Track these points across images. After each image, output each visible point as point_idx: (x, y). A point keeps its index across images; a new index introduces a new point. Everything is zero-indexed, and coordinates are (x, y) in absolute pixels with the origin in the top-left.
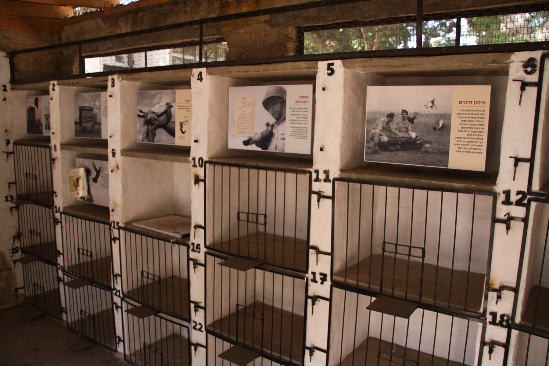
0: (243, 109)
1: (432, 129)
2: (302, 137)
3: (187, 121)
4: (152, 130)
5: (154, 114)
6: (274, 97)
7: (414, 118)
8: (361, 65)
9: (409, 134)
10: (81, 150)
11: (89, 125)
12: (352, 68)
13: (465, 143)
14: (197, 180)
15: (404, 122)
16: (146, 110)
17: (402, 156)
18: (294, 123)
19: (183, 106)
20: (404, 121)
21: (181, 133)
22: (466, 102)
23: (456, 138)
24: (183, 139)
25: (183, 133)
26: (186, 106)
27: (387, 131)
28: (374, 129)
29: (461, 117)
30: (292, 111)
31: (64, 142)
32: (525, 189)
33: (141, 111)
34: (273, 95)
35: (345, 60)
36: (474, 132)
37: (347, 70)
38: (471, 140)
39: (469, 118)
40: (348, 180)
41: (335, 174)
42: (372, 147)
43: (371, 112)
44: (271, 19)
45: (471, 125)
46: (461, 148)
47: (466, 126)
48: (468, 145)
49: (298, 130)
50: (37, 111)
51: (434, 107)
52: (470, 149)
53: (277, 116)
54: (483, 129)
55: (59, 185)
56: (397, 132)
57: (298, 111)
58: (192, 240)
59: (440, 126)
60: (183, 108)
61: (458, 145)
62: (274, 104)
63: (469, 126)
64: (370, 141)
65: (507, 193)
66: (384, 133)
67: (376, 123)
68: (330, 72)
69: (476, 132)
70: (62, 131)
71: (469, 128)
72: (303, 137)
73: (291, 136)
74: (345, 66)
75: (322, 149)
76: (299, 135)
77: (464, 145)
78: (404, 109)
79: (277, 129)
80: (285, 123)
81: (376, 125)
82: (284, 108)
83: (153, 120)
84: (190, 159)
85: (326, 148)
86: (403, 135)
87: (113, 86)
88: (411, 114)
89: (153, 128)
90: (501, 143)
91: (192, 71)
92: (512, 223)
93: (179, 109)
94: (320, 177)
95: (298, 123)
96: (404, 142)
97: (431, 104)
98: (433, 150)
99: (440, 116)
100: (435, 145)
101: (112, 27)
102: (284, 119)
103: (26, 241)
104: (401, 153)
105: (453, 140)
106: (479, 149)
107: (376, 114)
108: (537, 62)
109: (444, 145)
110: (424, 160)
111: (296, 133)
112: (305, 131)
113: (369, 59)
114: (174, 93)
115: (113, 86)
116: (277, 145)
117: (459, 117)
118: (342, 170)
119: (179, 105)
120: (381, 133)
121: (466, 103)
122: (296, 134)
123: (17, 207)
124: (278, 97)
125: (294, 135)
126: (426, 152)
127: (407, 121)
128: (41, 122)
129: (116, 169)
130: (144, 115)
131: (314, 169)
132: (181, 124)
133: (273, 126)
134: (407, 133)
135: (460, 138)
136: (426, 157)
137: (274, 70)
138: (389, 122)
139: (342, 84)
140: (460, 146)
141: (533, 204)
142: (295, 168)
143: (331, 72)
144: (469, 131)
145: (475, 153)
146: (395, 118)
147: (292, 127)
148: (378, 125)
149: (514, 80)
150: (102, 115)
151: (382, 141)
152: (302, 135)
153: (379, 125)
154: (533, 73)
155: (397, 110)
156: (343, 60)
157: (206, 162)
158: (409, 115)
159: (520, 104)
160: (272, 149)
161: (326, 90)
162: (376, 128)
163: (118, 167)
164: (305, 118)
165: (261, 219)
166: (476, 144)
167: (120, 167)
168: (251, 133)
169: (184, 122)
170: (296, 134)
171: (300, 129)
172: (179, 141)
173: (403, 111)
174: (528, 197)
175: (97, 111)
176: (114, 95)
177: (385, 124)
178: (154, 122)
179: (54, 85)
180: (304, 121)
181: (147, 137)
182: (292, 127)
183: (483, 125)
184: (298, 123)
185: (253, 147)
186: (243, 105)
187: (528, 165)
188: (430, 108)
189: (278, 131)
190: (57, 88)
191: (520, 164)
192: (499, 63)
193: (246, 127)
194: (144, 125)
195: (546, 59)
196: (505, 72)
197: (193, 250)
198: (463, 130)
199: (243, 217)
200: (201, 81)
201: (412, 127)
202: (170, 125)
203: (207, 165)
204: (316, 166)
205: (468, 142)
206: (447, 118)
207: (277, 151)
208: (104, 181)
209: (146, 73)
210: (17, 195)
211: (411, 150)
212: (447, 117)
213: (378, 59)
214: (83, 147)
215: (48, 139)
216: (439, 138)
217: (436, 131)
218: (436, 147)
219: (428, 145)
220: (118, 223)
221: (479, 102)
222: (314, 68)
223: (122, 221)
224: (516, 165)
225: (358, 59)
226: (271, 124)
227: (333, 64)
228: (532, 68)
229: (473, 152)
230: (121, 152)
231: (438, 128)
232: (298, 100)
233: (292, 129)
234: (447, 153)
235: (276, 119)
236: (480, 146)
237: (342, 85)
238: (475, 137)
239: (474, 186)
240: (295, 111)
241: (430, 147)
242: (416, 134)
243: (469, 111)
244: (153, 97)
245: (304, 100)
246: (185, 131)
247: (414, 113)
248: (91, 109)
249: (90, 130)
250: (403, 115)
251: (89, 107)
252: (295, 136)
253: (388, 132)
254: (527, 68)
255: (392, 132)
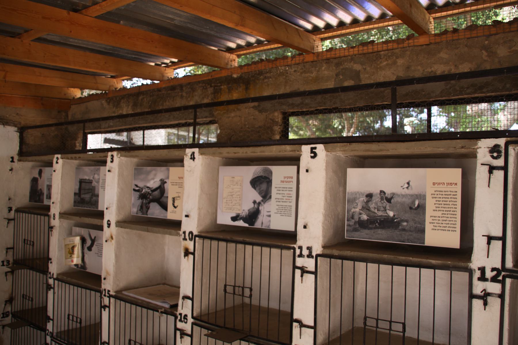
0: (232, 187)
1: (408, 209)
2: (286, 215)
3: (179, 197)
5: (148, 189)
6: (261, 177)
7: (392, 198)
8: (342, 149)
9: (387, 213)
10: (78, 219)
11: (87, 197)
12: (333, 152)
13: (440, 222)
14: (187, 253)
15: (383, 202)
16: (141, 185)
17: (381, 234)
18: (279, 202)
19: (176, 183)
20: (382, 200)
21: (173, 207)
22: (439, 184)
23: (431, 216)
24: (174, 213)
25: (175, 207)
26: (179, 183)
27: (366, 210)
28: (354, 208)
29: (435, 198)
30: (277, 190)
31: (62, 211)
32: (499, 266)
33: (137, 186)
34: (260, 175)
35: (327, 145)
36: (448, 211)
37: (329, 153)
38: (445, 219)
39: (443, 198)
40: (330, 257)
41: (318, 250)
42: (353, 225)
43: (351, 193)
44: (259, 106)
45: (445, 204)
46: (436, 226)
47: (440, 206)
48: (443, 224)
49: (283, 208)
50: (40, 182)
51: (409, 188)
52: (445, 227)
53: (263, 194)
54: (456, 208)
55: (55, 252)
56: (376, 211)
57: (283, 190)
58: (180, 310)
59: (416, 206)
60: (176, 184)
61: (433, 223)
62: (261, 183)
63: (443, 206)
64: (351, 219)
65: (482, 270)
66: (363, 211)
67: (356, 203)
68: (313, 155)
69: (450, 211)
70: (62, 202)
71: (443, 207)
72: (288, 215)
73: (276, 213)
74: (327, 150)
75: (305, 227)
76: (284, 213)
77: (439, 223)
78: (382, 190)
79: (263, 207)
80: (271, 201)
81: (356, 204)
82: (270, 188)
83: (148, 195)
84: (181, 232)
85: (310, 226)
86: (382, 214)
87: (112, 162)
88: (388, 195)
89: (147, 202)
90: (474, 222)
91: (185, 151)
92: (489, 299)
93: (172, 185)
94: (303, 253)
95: (283, 202)
96: (383, 220)
97: (406, 185)
98: (410, 228)
99: (415, 196)
100: (412, 223)
101: (115, 108)
102: (270, 197)
103: (17, 305)
104: (380, 231)
105: (428, 219)
106: (453, 227)
107: (356, 195)
108: (502, 148)
109: (420, 224)
110: (402, 237)
111: (281, 210)
112: (289, 209)
113: (349, 144)
114: (168, 170)
115: (112, 162)
116: (263, 222)
117: (433, 198)
118: (324, 247)
119: (172, 181)
120: (361, 211)
121: (439, 184)
122: (281, 211)
123: (12, 272)
124: (265, 176)
125: (280, 212)
126: (404, 230)
127: (385, 201)
128: (43, 192)
129: (110, 239)
130: (139, 189)
131: (298, 246)
132: (174, 200)
133: (259, 204)
134: (385, 212)
135: (435, 217)
136: (403, 235)
137: (261, 152)
138: (368, 202)
139: (325, 166)
140: (435, 225)
141: (508, 281)
142: (280, 244)
143: (314, 155)
144: (443, 211)
145: (449, 231)
146: (373, 198)
147: (277, 205)
148: (358, 204)
149: (482, 164)
150: (100, 188)
151: (362, 220)
152: (287, 213)
153: (359, 204)
154: (499, 158)
155: (375, 190)
156: (325, 145)
157: (196, 236)
158: (386, 195)
159: (489, 186)
160: (258, 225)
161: (309, 171)
162: (356, 207)
163: (112, 238)
164: (289, 197)
165: (247, 292)
166: (450, 222)
167: (114, 237)
168: (239, 210)
169: (176, 197)
170: (281, 211)
171: (285, 207)
172: (171, 215)
173: (381, 192)
174: (503, 273)
175: (96, 184)
176: (113, 170)
177: (364, 203)
179: (57, 158)
180: (288, 199)
181: (141, 210)
182: (277, 205)
183: (456, 205)
184: (283, 202)
185: (241, 223)
186: (232, 183)
187: (500, 242)
188: (406, 188)
189: (264, 209)
190: (60, 161)
191: (493, 242)
192: (468, 148)
193: (234, 204)
194: (139, 199)
195: (509, 146)
196: (474, 156)
197: (180, 320)
198: (438, 209)
199: (230, 289)
200: (194, 160)
201: (389, 207)
202: (163, 199)
203: (197, 238)
204: (299, 243)
205: (443, 220)
206: (422, 198)
207: (263, 227)
208: (99, 250)
209: (143, 151)
210: (14, 260)
211: (389, 228)
212: (422, 197)
213: (357, 144)
214: (80, 217)
215: (48, 208)
216: (416, 217)
217: (412, 210)
218: (413, 225)
219: (405, 224)
220: (109, 291)
221: (451, 184)
222: (298, 151)
223: (113, 290)
224: (489, 243)
225: (339, 144)
226: (257, 202)
227: (315, 148)
228: (497, 153)
229: (448, 230)
230: (116, 223)
231: (414, 208)
232: (283, 180)
233: (277, 207)
234: (423, 231)
235: (263, 197)
236: (454, 224)
237: (324, 167)
238: (449, 216)
239: (450, 262)
240: (280, 190)
241: (407, 226)
242: (394, 213)
243: (442, 191)
244: (148, 173)
245: (289, 180)
246: (177, 206)
247: (391, 194)
248: (90, 182)
249: (88, 201)
250: (381, 196)
251: (89, 179)
252: (280, 213)
253: (368, 211)
254: (493, 153)
255: (371, 211)
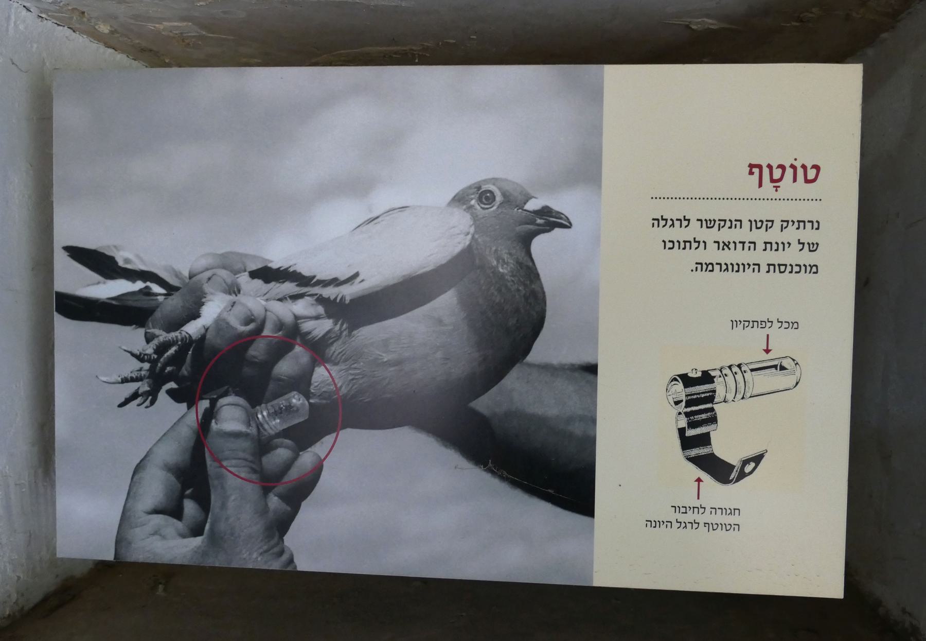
4: (263, 446)
5: (289, 287)
83: (281, 349)
89: (276, 425)
130: (146, 292)
178: (285, 367)
181: (190, 507)
